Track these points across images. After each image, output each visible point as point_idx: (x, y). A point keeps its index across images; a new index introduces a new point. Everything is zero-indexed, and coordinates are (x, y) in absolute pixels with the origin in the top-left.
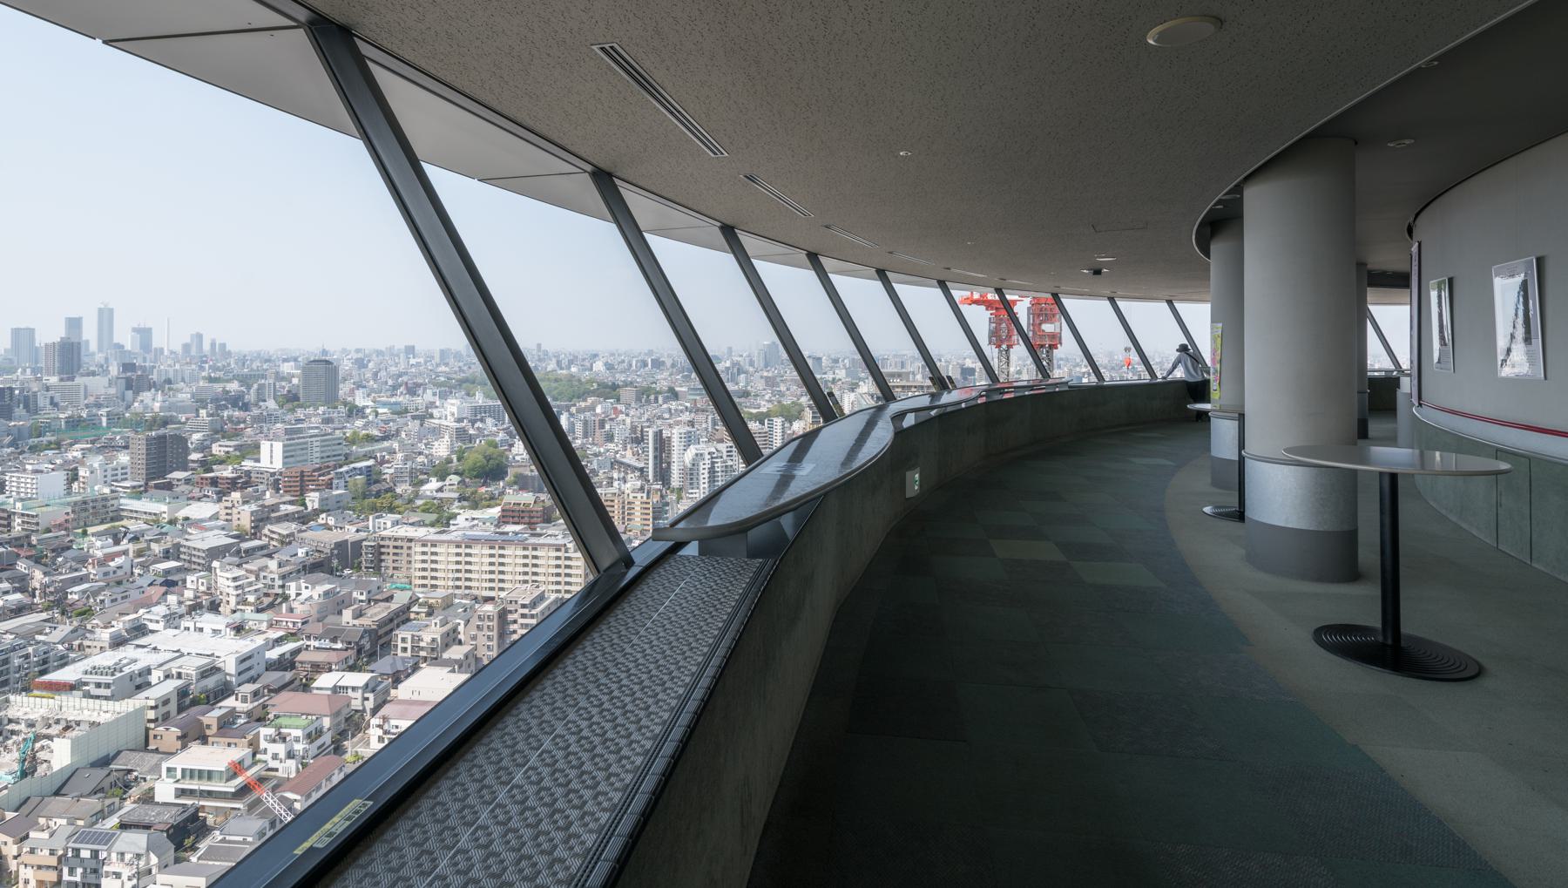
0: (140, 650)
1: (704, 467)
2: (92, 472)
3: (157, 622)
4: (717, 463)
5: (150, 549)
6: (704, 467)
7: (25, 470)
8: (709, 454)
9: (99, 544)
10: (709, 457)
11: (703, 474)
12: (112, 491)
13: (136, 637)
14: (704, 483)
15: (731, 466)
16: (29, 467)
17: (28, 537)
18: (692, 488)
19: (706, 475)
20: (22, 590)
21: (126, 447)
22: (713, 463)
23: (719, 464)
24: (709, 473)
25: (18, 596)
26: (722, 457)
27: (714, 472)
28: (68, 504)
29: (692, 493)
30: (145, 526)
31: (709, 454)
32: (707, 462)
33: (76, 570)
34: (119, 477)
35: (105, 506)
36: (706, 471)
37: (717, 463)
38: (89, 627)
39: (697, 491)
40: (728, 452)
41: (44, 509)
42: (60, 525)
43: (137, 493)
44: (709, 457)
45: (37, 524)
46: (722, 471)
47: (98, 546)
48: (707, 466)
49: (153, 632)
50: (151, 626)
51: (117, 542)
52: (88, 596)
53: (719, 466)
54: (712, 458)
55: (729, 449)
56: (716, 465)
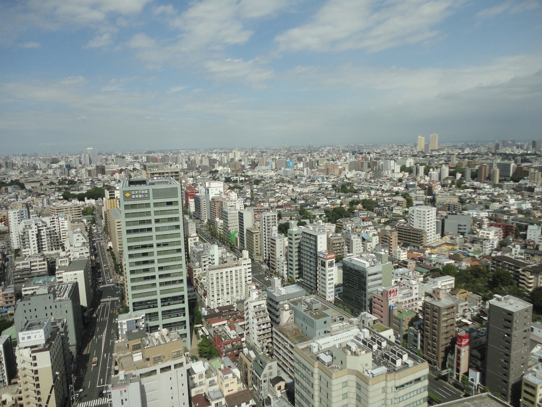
1: (33, 233)
4: (43, 230)
6: (33, 233)
8: (36, 224)
10: (36, 227)
11: (32, 238)
14: (34, 244)
15: (53, 231)
18: (25, 248)
19: (35, 239)
22: (39, 231)
23: (44, 231)
24: (37, 237)
26: (46, 226)
27: (41, 236)
29: (26, 252)
31: (36, 224)
32: (34, 230)
36: (35, 236)
37: (43, 230)
39: (30, 250)
40: (51, 222)
44: (36, 227)
46: (47, 235)
48: (35, 233)
53: (44, 233)
54: (38, 227)
55: (52, 220)
56: (42, 231)
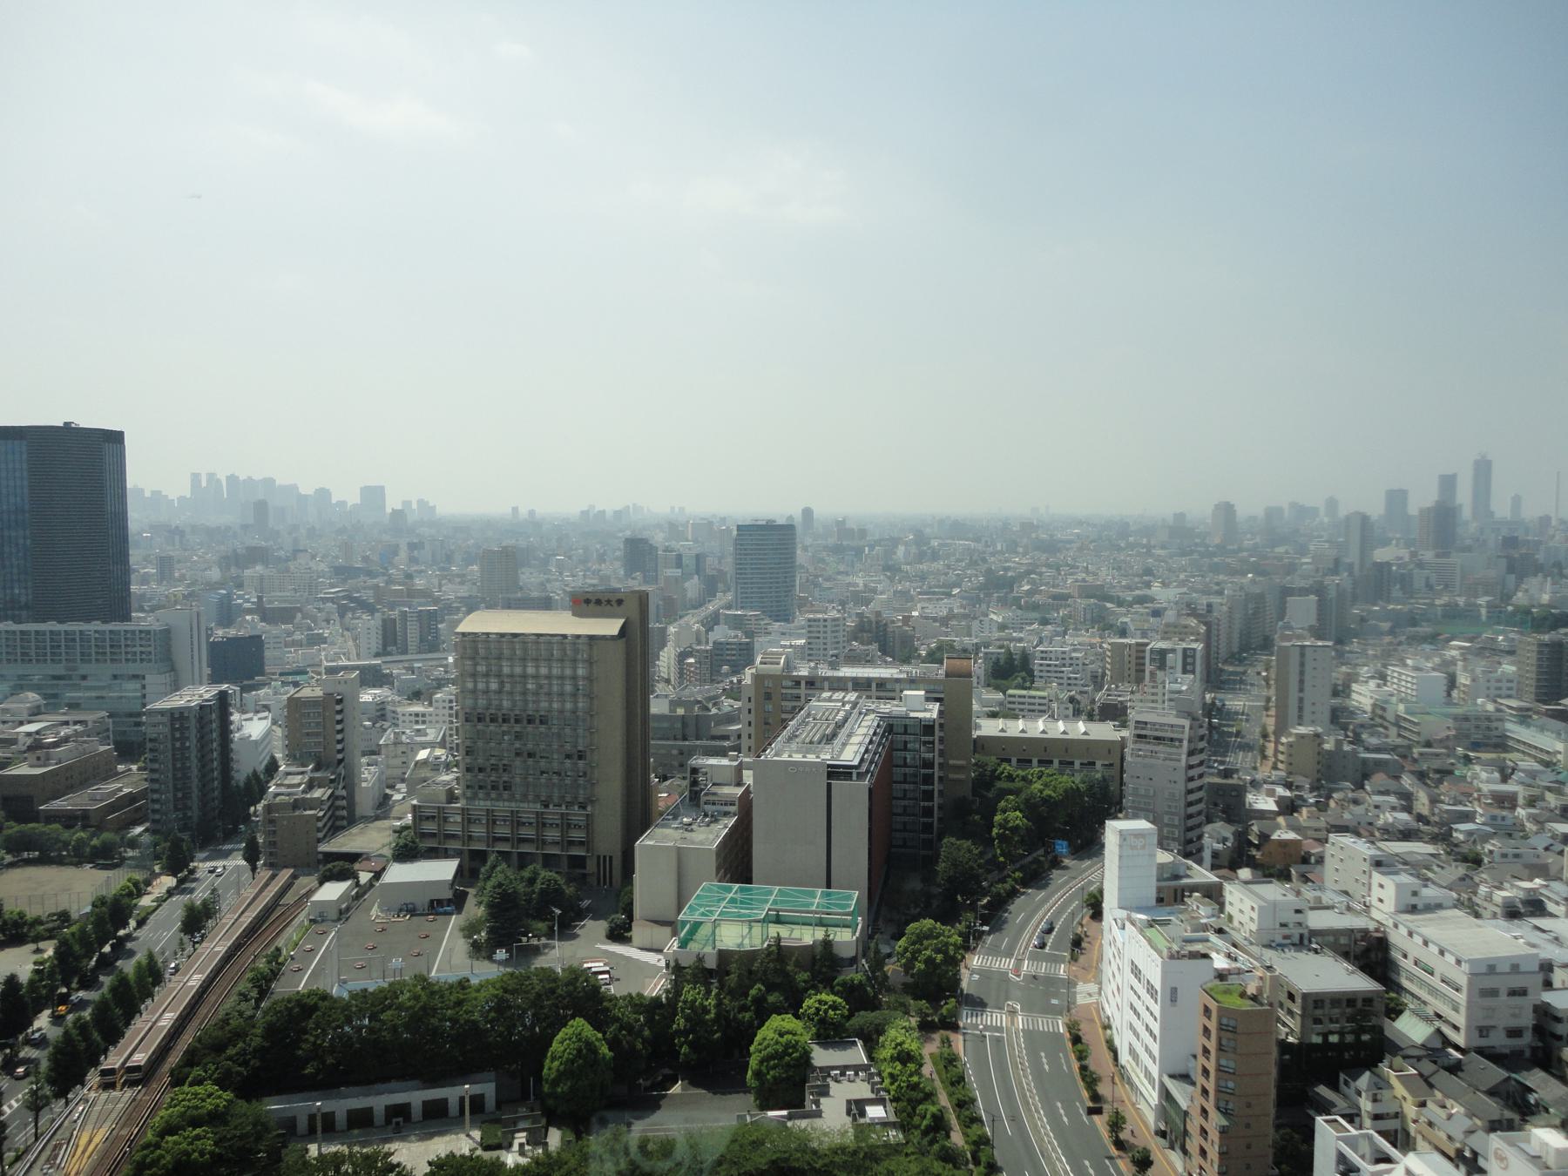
0: (1538, 933)
2: (1474, 680)
3: (1557, 903)
5: (1543, 799)
7: (1405, 665)
9: (1484, 775)
12: (1498, 710)
13: (1533, 915)
16: (1409, 662)
17: (1409, 747)
20: (1408, 809)
21: (1511, 653)
25: (1404, 816)
28: (1447, 715)
30: (1537, 766)
33: (1460, 803)
34: (1504, 692)
35: (1488, 728)
38: (1477, 879)
41: (1427, 717)
42: (1441, 741)
43: (1524, 717)
45: (1418, 734)
47: (1484, 779)
49: (1552, 915)
50: (1551, 907)
51: (1505, 779)
52: (1474, 842)
